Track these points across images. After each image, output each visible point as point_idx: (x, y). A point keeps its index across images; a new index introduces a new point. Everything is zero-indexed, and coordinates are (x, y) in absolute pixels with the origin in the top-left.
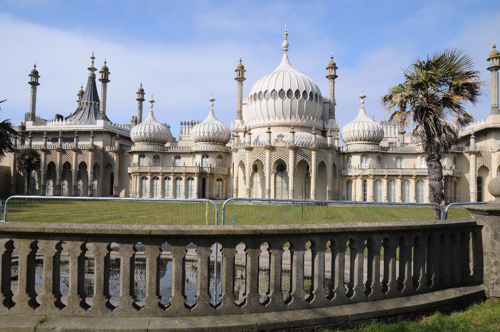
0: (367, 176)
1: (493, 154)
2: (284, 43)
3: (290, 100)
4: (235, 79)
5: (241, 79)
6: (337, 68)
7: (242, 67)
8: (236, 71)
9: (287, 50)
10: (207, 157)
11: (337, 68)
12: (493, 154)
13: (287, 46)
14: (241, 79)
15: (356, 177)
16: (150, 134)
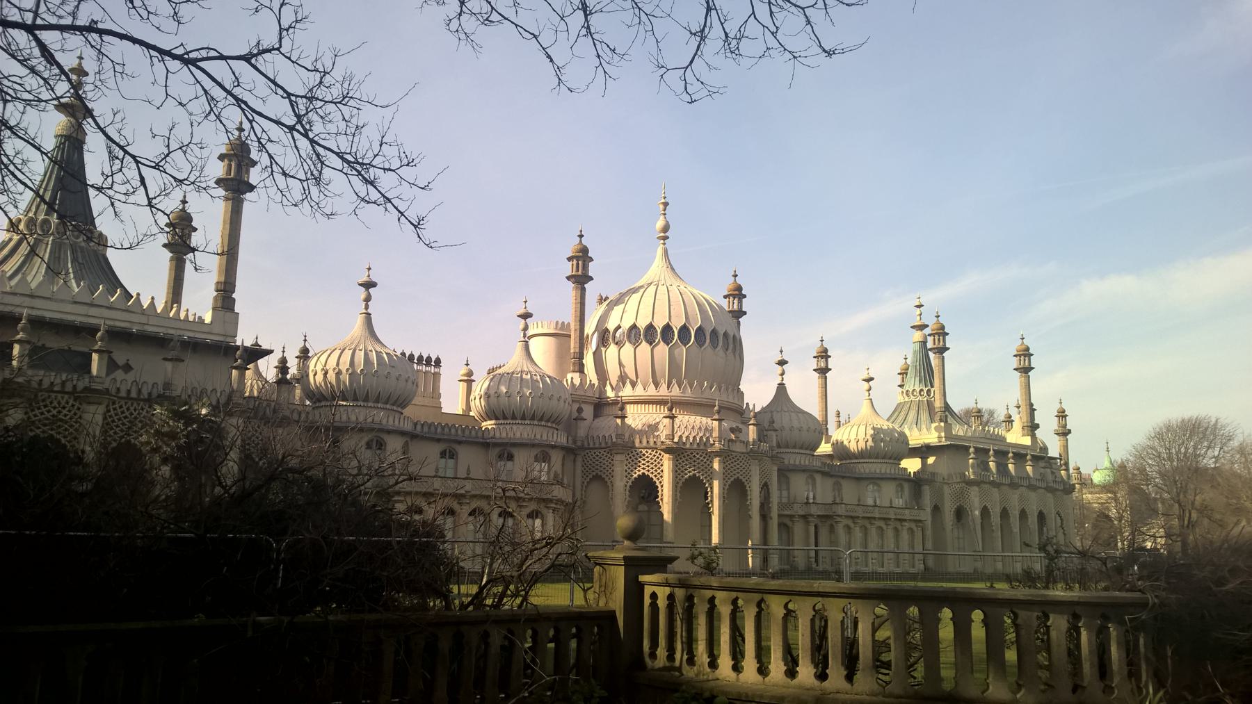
0: (791, 517)
1: (946, 487)
2: (660, 224)
3: (667, 348)
4: (568, 278)
5: (581, 280)
6: (745, 296)
7: (584, 250)
8: (570, 259)
9: (665, 238)
10: (545, 458)
11: (745, 296)
12: (947, 490)
13: (666, 229)
14: (581, 280)
15: (804, 517)
16: (352, 375)
